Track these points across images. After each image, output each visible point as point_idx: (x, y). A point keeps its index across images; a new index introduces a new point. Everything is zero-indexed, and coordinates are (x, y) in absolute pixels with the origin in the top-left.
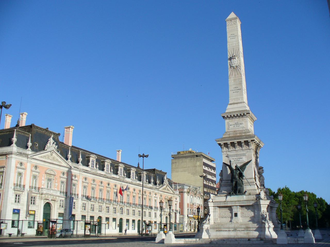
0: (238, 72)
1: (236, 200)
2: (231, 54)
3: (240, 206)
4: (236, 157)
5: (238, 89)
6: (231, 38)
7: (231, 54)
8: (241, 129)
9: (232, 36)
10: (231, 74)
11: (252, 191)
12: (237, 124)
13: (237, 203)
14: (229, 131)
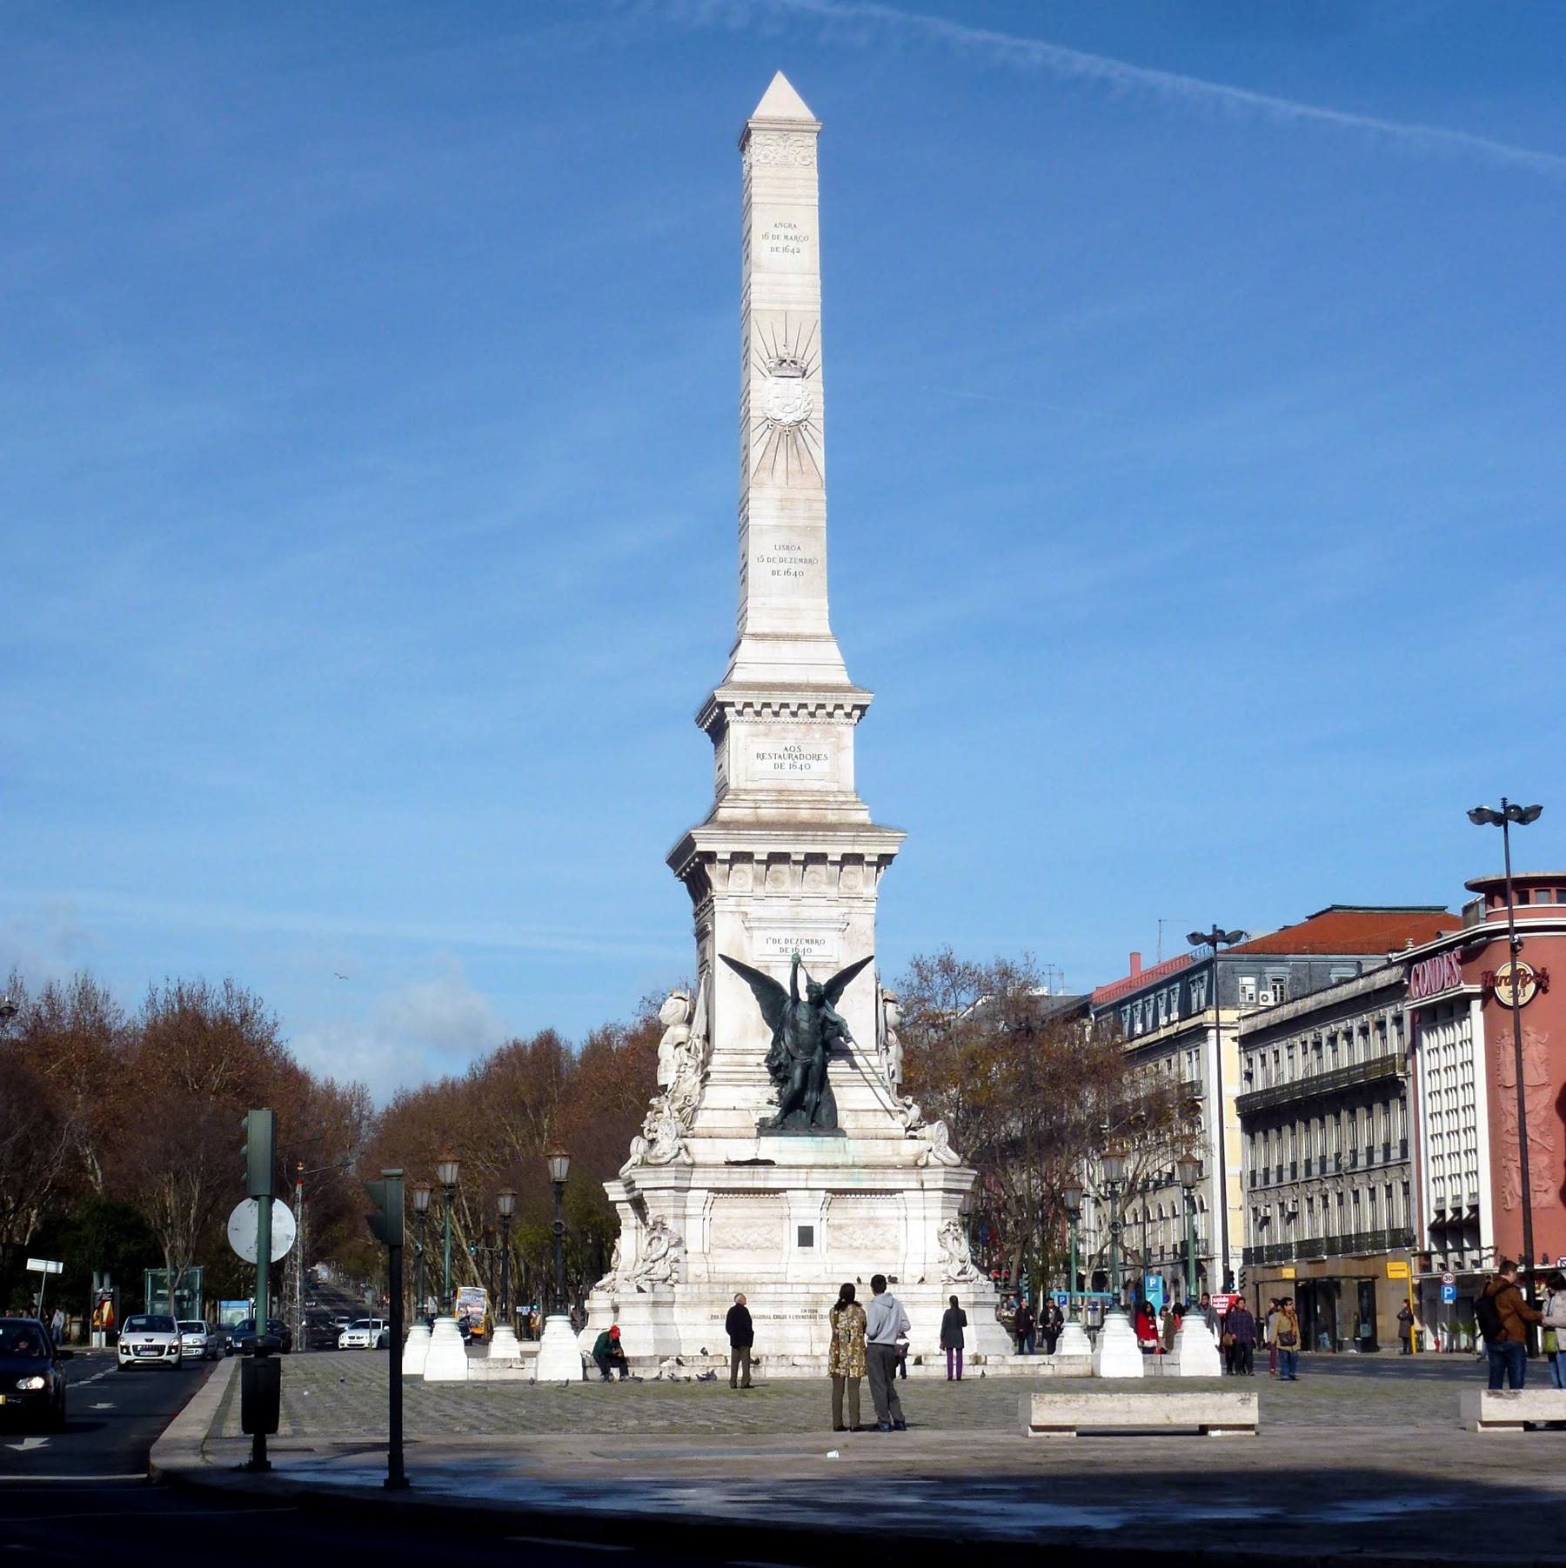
0: (806, 460)
1: (810, 1161)
2: (770, 344)
3: (828, 1190)
4: (788, 934)
5: (801, 560)
6: (776, 243)
7: (770, 344)
8: (817, 786)
9: (781, 231)
10: (768, 461)
11: (875, 1116)
12: (794, 754)
13: (817, 1176)
14: (750, 786)
